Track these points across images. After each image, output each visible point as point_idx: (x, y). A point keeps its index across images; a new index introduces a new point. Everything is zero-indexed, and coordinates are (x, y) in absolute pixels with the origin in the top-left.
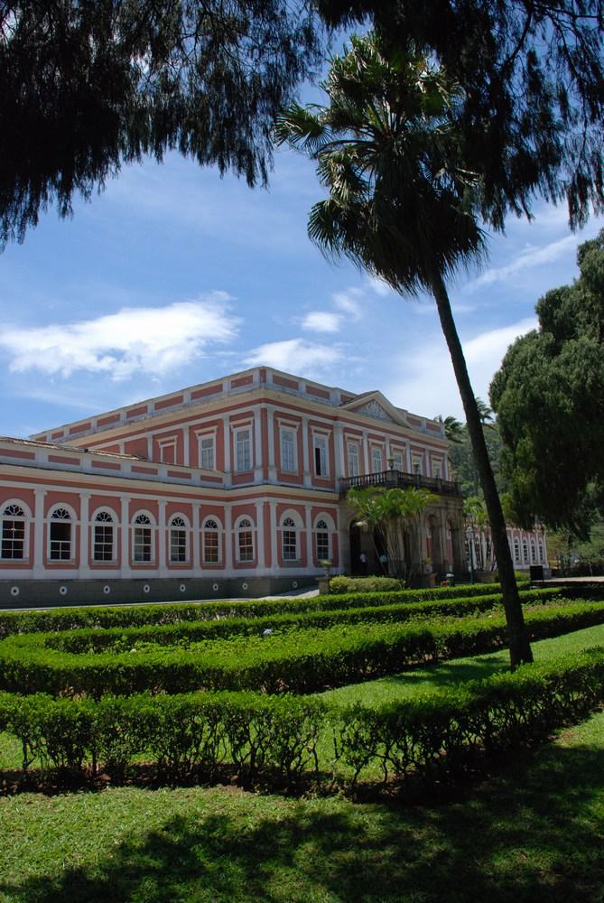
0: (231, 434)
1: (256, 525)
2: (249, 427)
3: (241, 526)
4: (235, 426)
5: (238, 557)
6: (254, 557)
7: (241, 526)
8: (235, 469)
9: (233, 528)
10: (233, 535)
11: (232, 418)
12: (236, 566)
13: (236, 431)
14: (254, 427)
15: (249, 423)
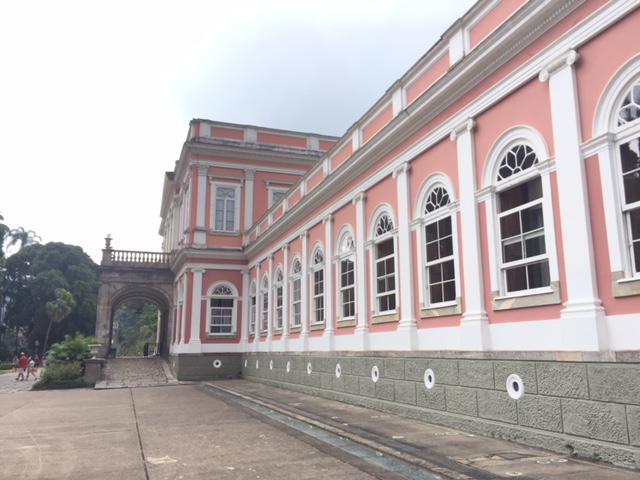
0: (209, 185)
1: (240, 294)
2: (238, 187)
3: (215, 292)
4: (214, 179)
5: (208, 329)
6: (234, 329)
7: (215, 292)
8: (212, 226)
9: (204, 292)
10: (203, 303)
11: (210, 169)
12: (205, 339)
13: (214, 185)
14: (243, 188)
15: (239, 181)
